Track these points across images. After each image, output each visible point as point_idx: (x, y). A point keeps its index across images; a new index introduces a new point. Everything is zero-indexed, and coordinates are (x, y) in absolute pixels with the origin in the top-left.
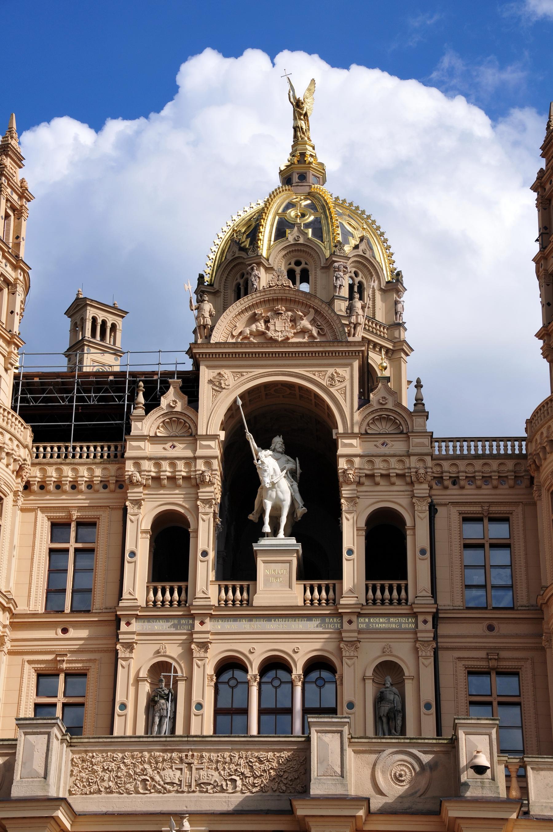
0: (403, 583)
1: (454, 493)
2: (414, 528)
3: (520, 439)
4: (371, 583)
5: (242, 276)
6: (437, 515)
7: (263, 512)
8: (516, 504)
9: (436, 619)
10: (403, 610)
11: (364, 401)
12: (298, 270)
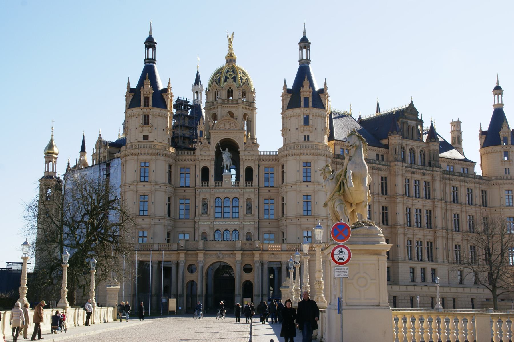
0: (252, 182)
1: (263, 162)
2: (255, 171)
3: (277, 151)
4: (246, 182)
5: (217, 89)
6: (260, 167)
7: (224, 166)
8: (275, 165)
9: (258, 189)
10: (252, 188)
12: (230, 90)
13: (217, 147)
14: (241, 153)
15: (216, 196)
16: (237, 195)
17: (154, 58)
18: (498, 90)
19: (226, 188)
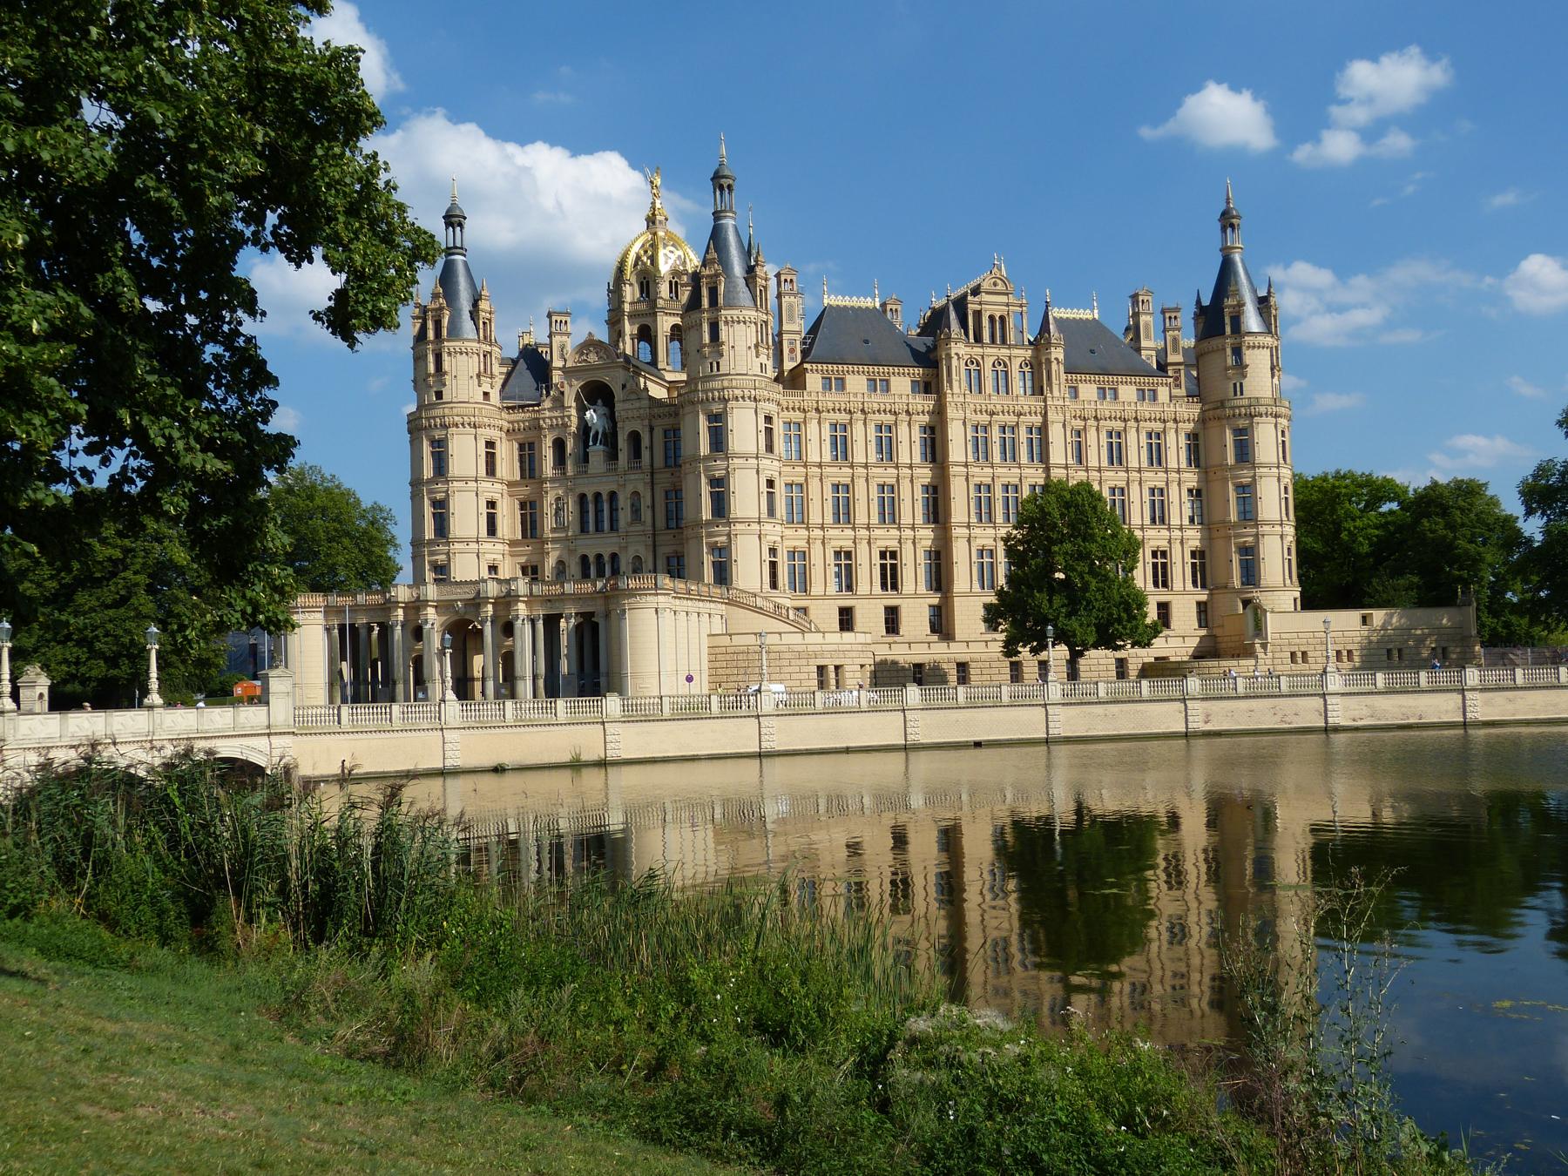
9: (652, 474)
11: (624, 386)
13: (578, 399)
14: (618, 407)
15: (579, 491)
16: (614, 487)
17: (459, 245)
18: (1227, 221)
19: (595, 476)
